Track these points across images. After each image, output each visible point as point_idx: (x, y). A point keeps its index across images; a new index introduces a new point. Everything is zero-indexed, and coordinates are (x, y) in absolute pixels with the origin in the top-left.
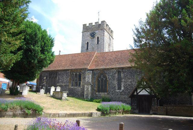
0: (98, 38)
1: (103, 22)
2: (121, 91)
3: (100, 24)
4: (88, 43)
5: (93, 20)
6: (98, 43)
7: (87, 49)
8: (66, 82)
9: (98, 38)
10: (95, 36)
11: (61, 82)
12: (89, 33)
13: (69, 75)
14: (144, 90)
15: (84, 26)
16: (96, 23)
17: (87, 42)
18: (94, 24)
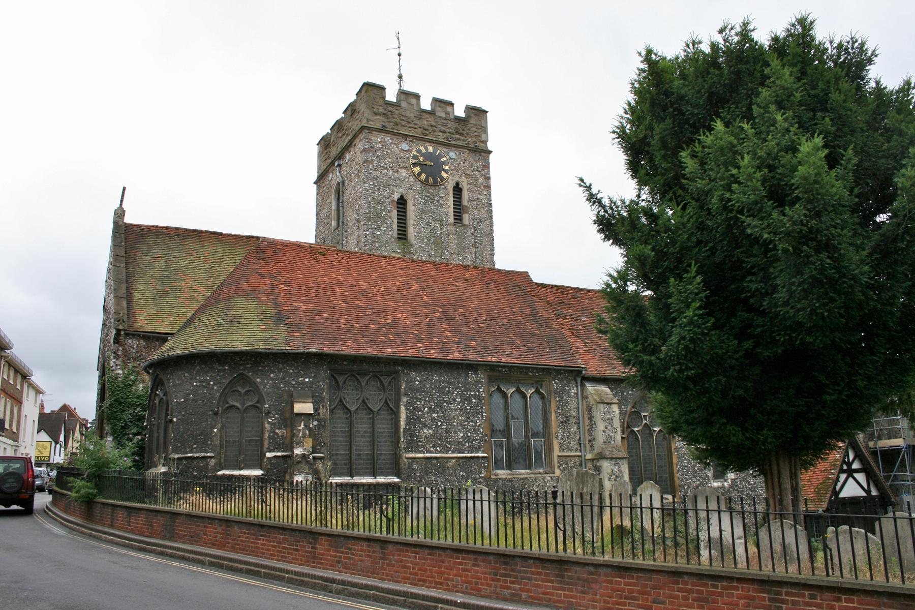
0: (458, 190)
1: (477, 114)
2: (726, 484)
3: (458, 119)
4: (402, 203)
5: (434, 81)
6: (458, 218)
7: (402, 235)
8: (466, 438)
9: (458, 190)
10: (444, 174)
11: (429, 439)
12: (405, 146)
13: (478, 397)
14: (851, 480)
15: (371, 91)
16: (436, 101)
17: (396, 196)
18: (426, 104)
